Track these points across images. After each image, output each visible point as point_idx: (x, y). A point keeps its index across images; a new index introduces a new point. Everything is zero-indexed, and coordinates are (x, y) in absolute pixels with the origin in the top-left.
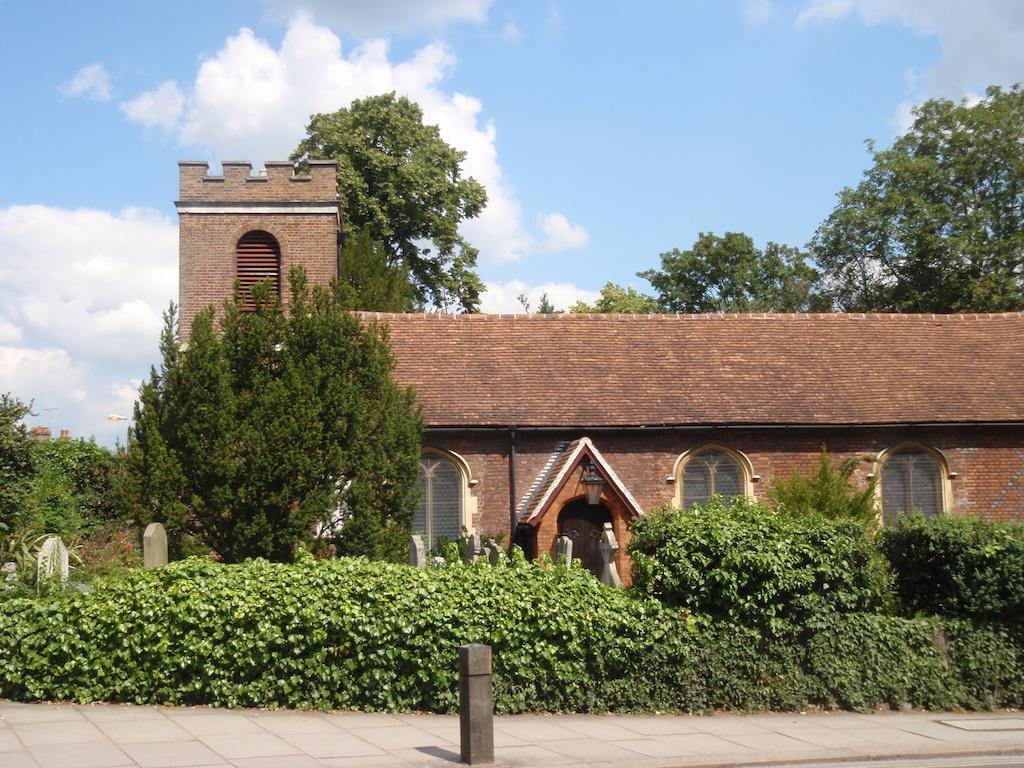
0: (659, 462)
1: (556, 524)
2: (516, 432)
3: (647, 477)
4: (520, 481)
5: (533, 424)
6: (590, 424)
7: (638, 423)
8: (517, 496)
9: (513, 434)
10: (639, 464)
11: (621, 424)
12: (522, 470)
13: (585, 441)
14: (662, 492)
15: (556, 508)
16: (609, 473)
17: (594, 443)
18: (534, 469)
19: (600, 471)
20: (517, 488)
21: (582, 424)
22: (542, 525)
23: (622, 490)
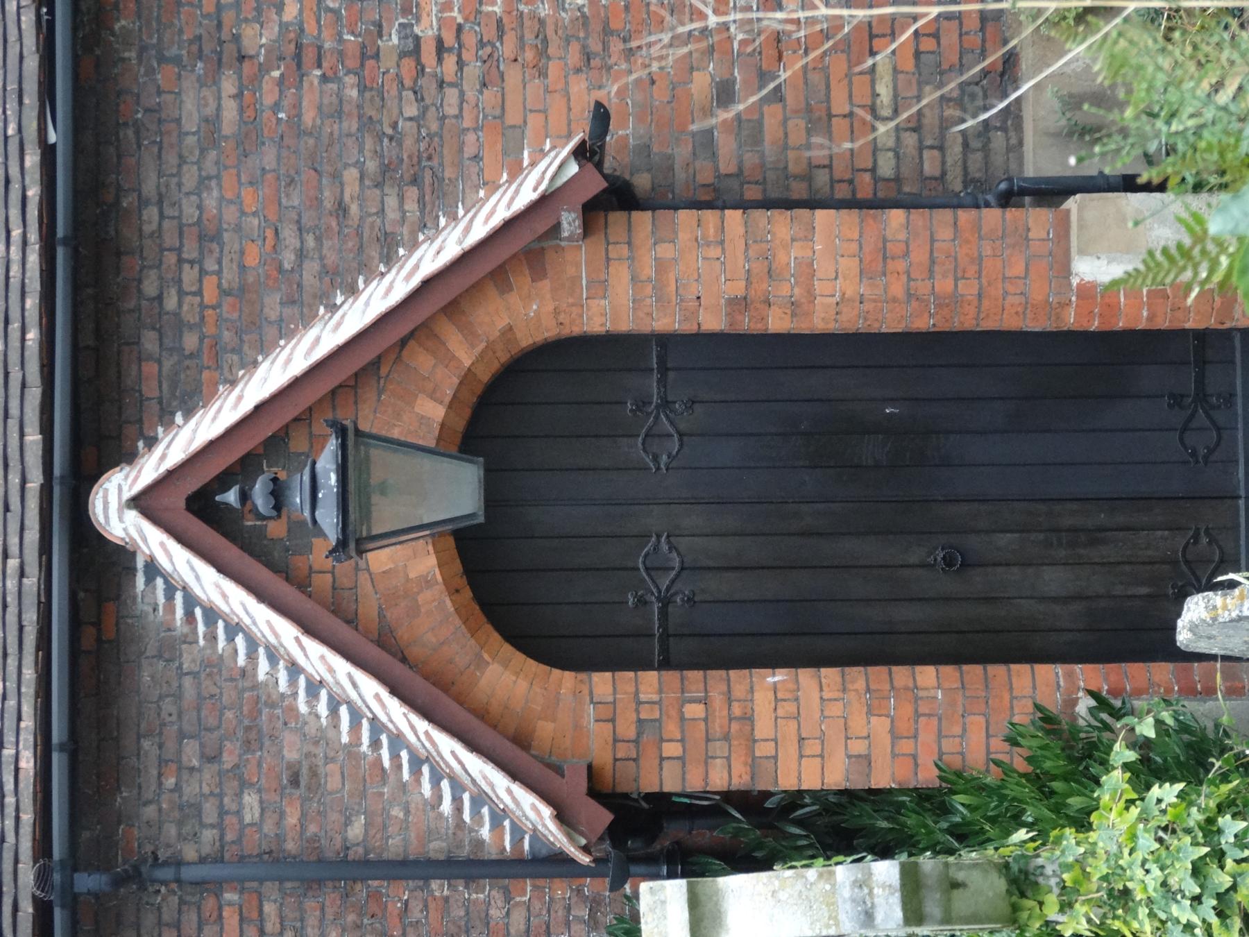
0: (259, 38)
1: (602, 682)
2: (74, 863)
3: (339, 114)
4: (356, 830)
5: (28, 763)
6: (34, 438)
7: (32, 159)
8: (436, 849)
9: (87, 882)
10: (269, 157)
11: (33, 258)
12: (292, 819)
13: (113, 506)
14: (427, 29)
15: (508, 678)
16: (299, 365)
17: (129, 457)
18: (291, 755)
19: (264, 445)
20: (394, 846)
21: (35, 481)
22: (601, 754)
23: (401, 290)
